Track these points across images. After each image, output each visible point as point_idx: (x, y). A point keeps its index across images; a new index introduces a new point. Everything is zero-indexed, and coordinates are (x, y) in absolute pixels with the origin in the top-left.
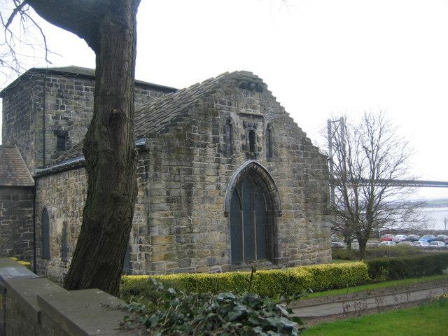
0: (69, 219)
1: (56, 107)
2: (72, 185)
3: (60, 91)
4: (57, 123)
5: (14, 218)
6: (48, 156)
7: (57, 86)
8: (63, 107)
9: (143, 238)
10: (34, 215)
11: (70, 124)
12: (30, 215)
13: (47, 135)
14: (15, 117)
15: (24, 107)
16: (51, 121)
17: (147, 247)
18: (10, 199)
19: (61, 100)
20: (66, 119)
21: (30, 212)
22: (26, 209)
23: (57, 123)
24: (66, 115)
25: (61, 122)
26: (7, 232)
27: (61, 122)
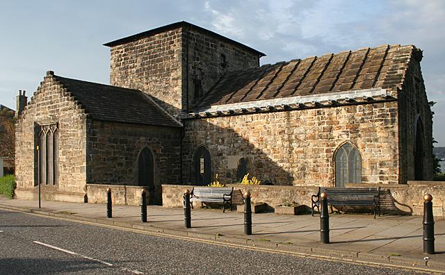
0: (253, 156)
1: (194, 58)
2: (257, 127)
3: (196, 44)
4: (195, 72)
5: (168, 155)
6: (190, 101)
7: (194, 40)
8: (198, 60)
9: (384, 169)
10: (181, 154)
11: (202, 74)
12: (178, 153)
13: (189, 82)
14: (138, 64)
15: (156, 56)
16: (191, 71)
17: (393, 177)
18: (165, 137)
19: (196, 51)
20: (200, 69)
21: (178, 150)
22: (176, 148)
23: (195, 72)
24: (200, 66)
25: (198, 72)
26: (163, 168)
27: (198, 72)
